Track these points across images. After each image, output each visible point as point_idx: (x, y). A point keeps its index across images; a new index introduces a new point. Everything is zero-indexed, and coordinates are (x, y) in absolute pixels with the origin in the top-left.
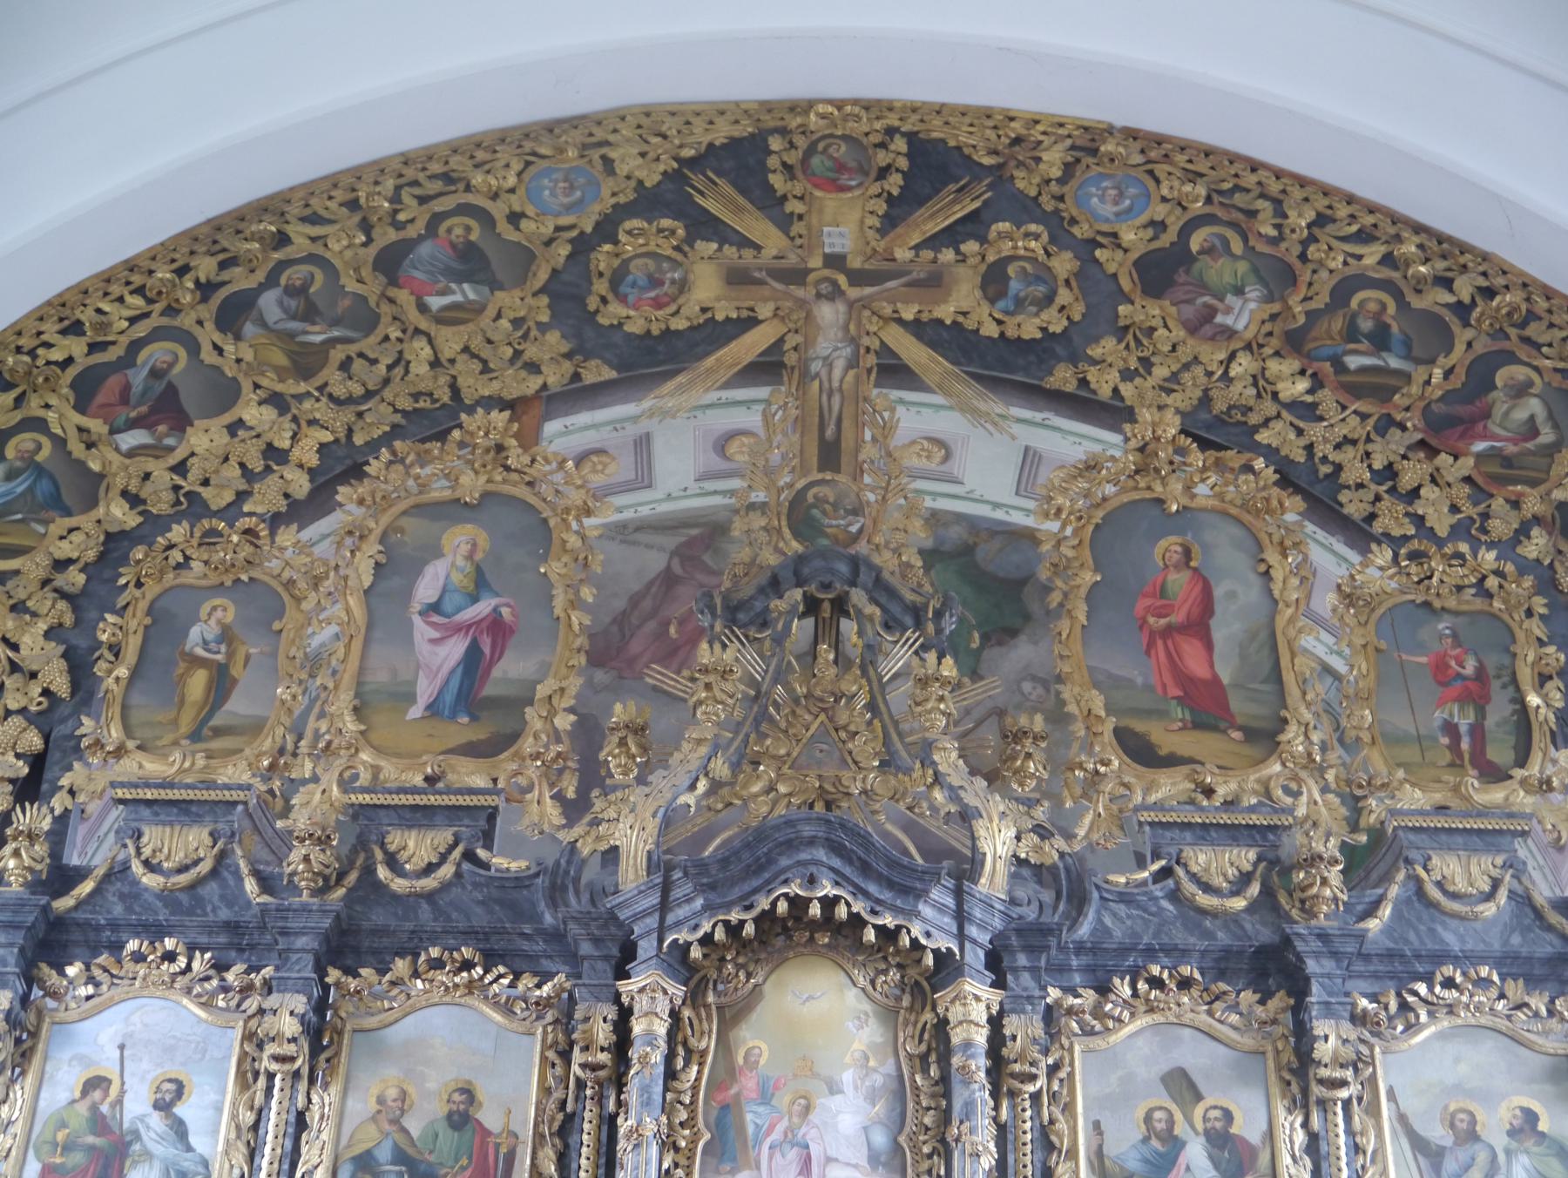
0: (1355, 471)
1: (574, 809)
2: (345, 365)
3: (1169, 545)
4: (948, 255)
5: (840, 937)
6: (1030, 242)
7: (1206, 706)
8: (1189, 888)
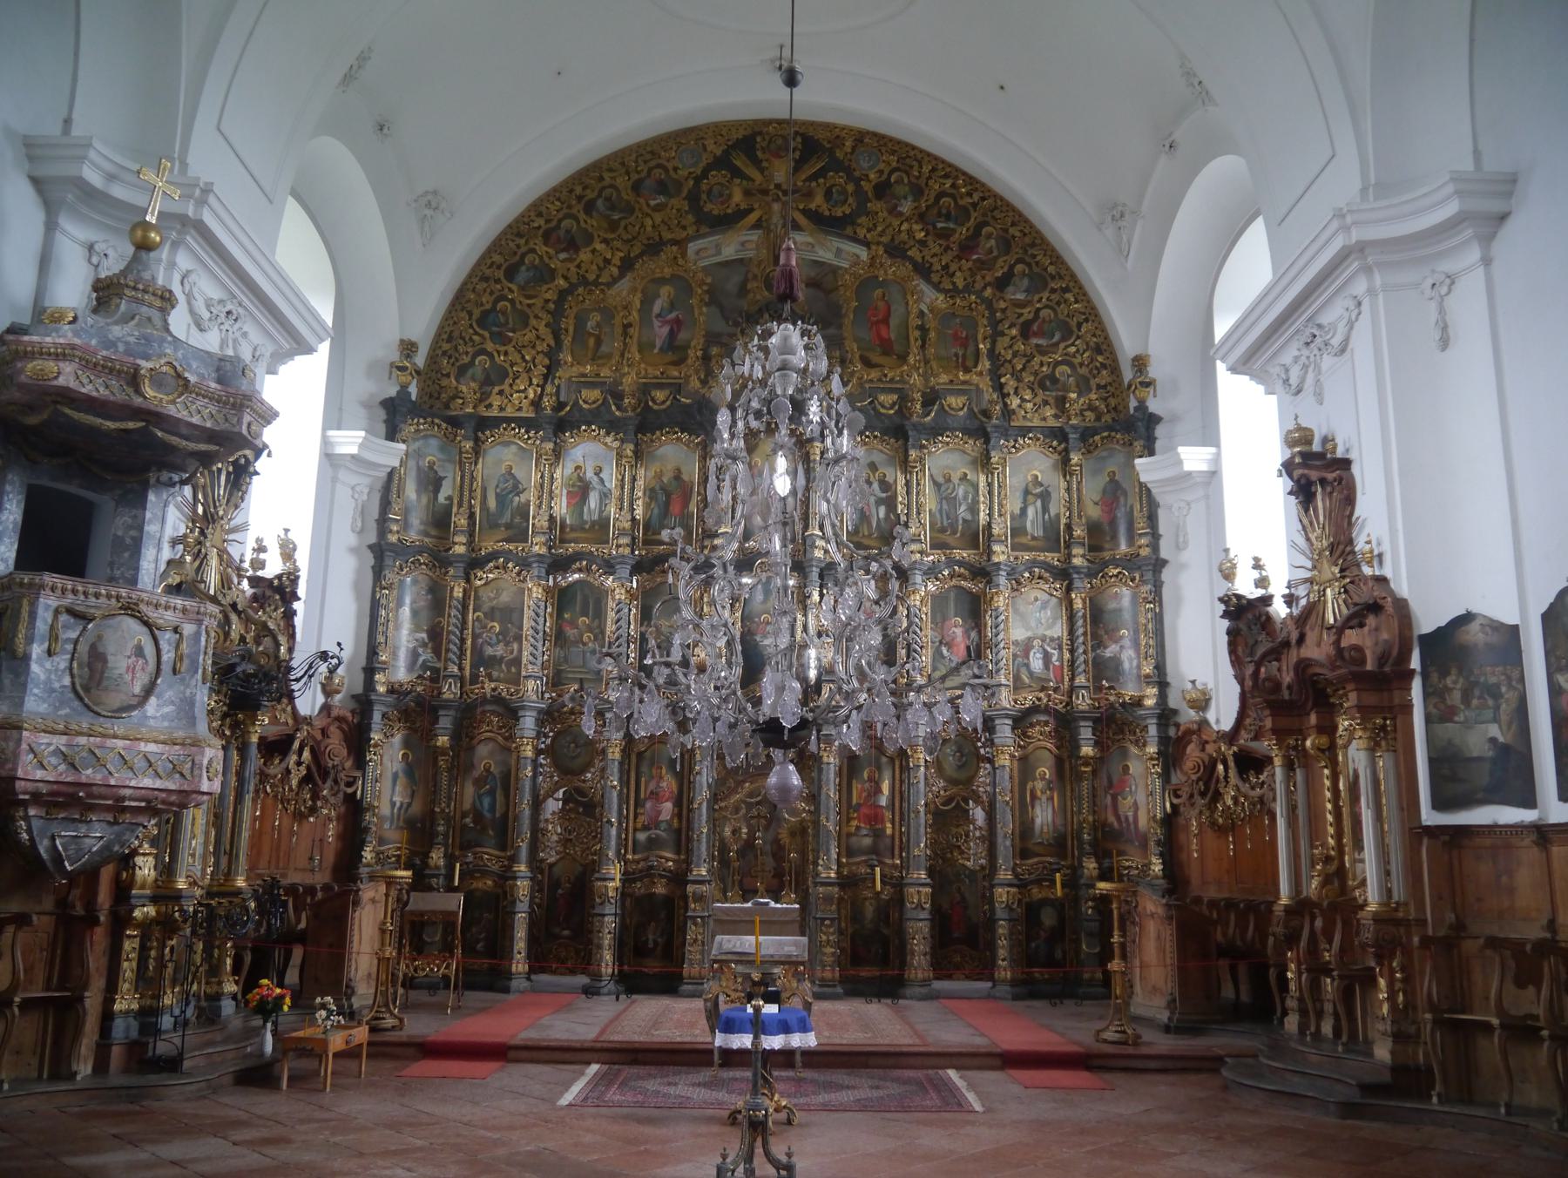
0: (937, 267)
1: (704, 382)
2: (625, 228)
3: (879, 292)
4: (814, 184)
6: (840, 179)
7: (886, 348)
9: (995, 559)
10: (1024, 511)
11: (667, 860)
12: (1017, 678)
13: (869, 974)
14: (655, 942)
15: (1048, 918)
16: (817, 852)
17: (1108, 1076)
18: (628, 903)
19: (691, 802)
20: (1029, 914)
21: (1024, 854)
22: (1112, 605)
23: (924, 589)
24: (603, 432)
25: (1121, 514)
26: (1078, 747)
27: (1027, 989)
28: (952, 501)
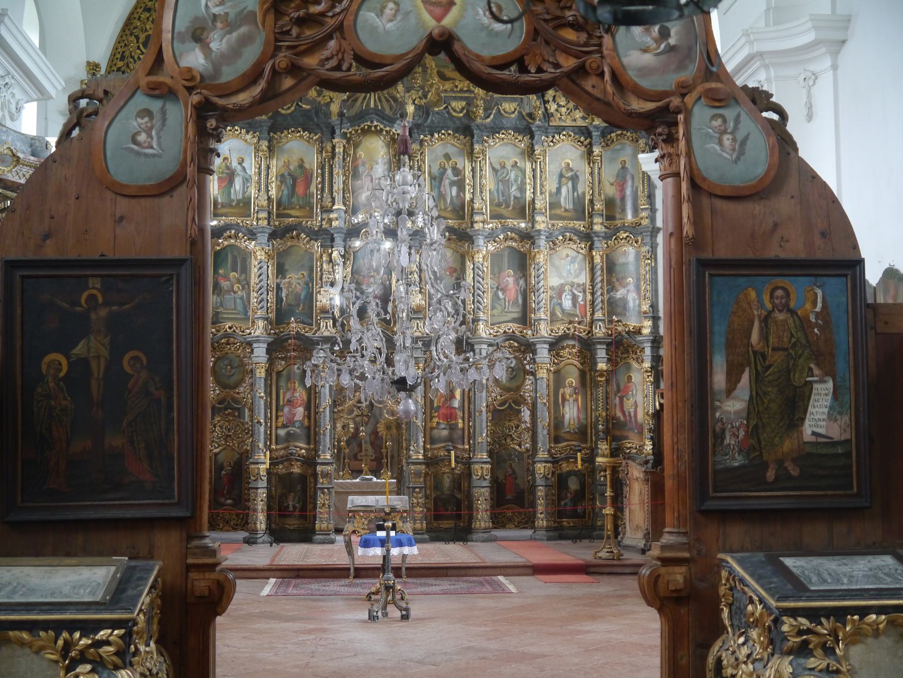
5: (379, 132)
8: (451, 111)
9: (538, 227)
10: (559, 190)
11: (301, 449)
12: (553, 314)
13: (447, 526)
14: (294, 507)
15: (573, 484)
16: (408, 441)
17: (597, 577)
18: (273, 481)
19: (317, 407)
20: (560, 482)
21: (557, 440)
22: (621, 260)
23: (484, 250)
24: (244, 131)
25: (628, 192)
26: (596, 364)
27: (558, 533)
28: (506, 183)
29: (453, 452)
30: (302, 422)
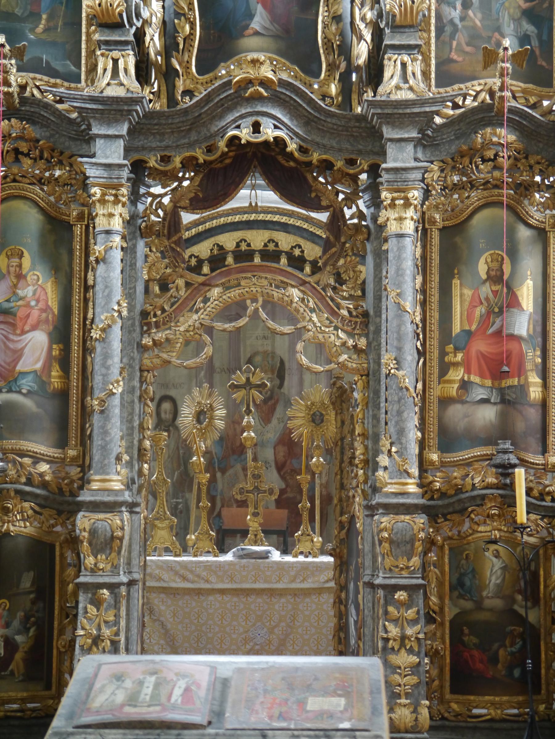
13: (494, 713)
19: (86, 329)
29: (520, 473)
30: (41, 379)
